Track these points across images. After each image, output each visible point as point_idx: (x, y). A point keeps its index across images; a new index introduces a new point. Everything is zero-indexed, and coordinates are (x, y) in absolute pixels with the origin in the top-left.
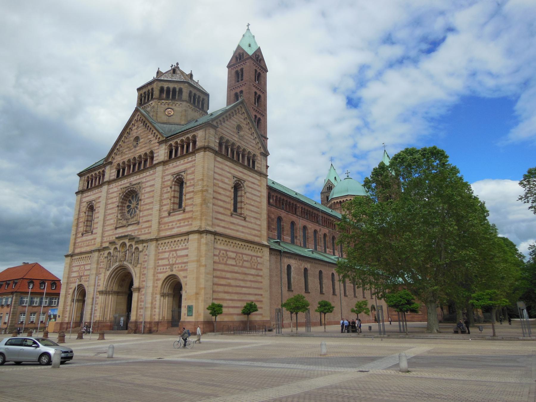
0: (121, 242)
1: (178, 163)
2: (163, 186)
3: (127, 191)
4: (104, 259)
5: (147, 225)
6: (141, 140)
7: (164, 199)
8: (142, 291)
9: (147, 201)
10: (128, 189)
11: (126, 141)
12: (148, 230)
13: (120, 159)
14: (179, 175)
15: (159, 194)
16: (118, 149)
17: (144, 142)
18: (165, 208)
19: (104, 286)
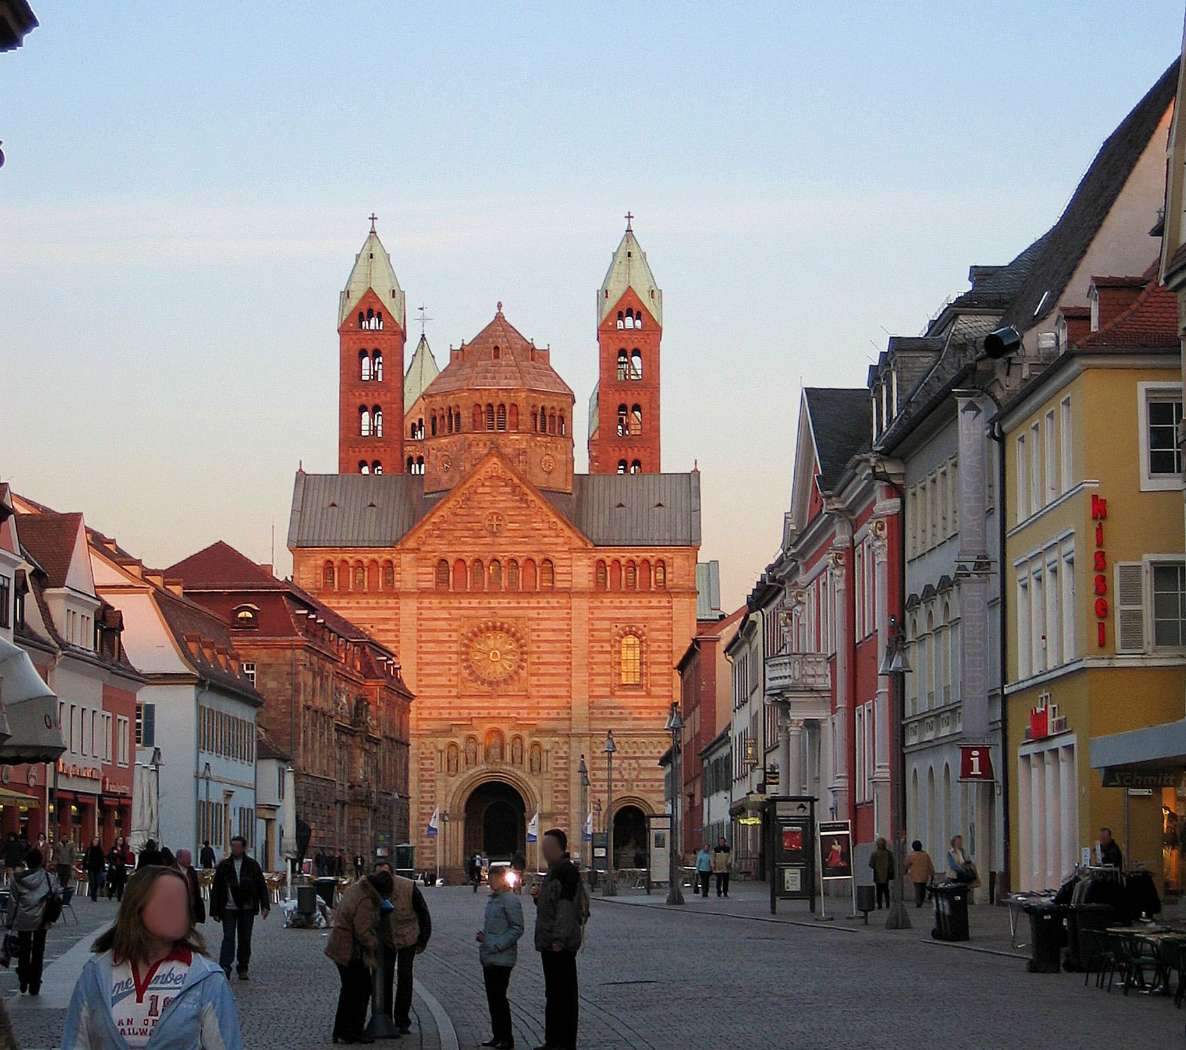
0: (489, 726)
1: (626, 602)
2: (591, 638)
3: (482, 626)
4: (432, 753)
5: (555, 705)
6: (510, 525)
7: (596, 663)
8: (557, 820)
9: (546, 658)
10: (486, 623)
11: (459, 511)
12: (558, 714)
13: (444, 548)
14: (629, 627)
15: (586, 652)
16: (434, 522)
17: (521, 533)
18: (599, 680)
19: (449, 805)
